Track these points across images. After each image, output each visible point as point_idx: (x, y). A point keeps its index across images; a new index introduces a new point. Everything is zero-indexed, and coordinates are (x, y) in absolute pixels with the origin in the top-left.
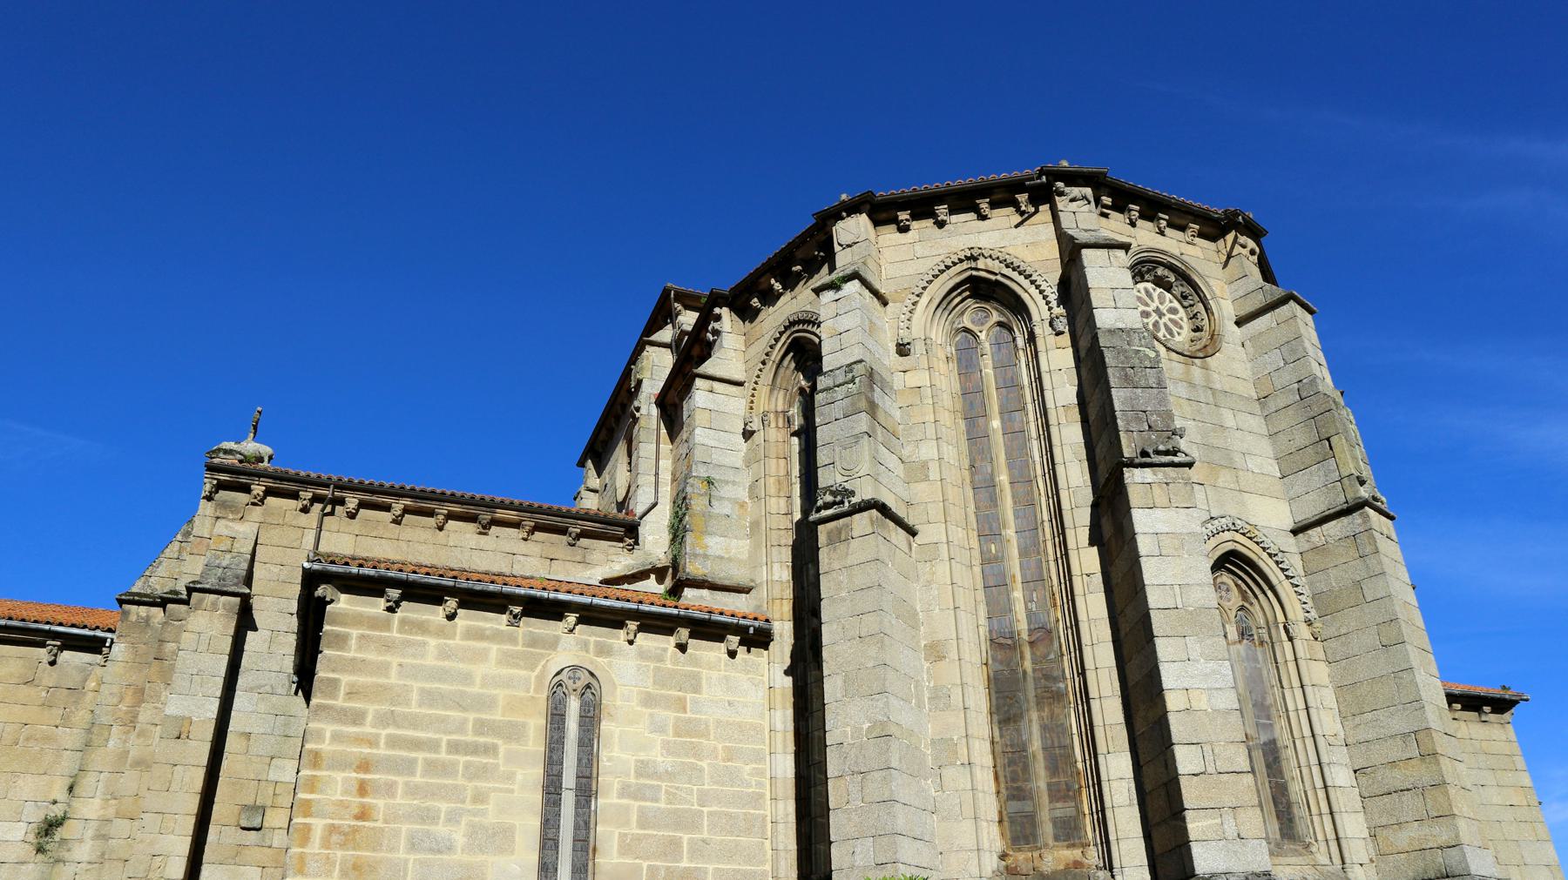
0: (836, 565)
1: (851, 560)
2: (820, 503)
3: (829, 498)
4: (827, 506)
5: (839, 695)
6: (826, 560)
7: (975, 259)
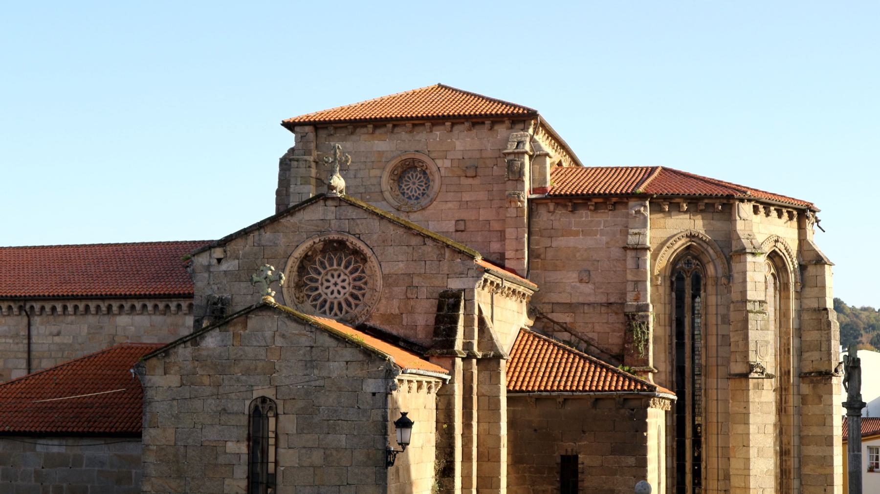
0: (757, 400)
1: (763, 399)
2: (755, 371)
3: (758, 370)
4: (756, 372)
5: (756, 456)
6: (753, 396)
7: (776, 241)
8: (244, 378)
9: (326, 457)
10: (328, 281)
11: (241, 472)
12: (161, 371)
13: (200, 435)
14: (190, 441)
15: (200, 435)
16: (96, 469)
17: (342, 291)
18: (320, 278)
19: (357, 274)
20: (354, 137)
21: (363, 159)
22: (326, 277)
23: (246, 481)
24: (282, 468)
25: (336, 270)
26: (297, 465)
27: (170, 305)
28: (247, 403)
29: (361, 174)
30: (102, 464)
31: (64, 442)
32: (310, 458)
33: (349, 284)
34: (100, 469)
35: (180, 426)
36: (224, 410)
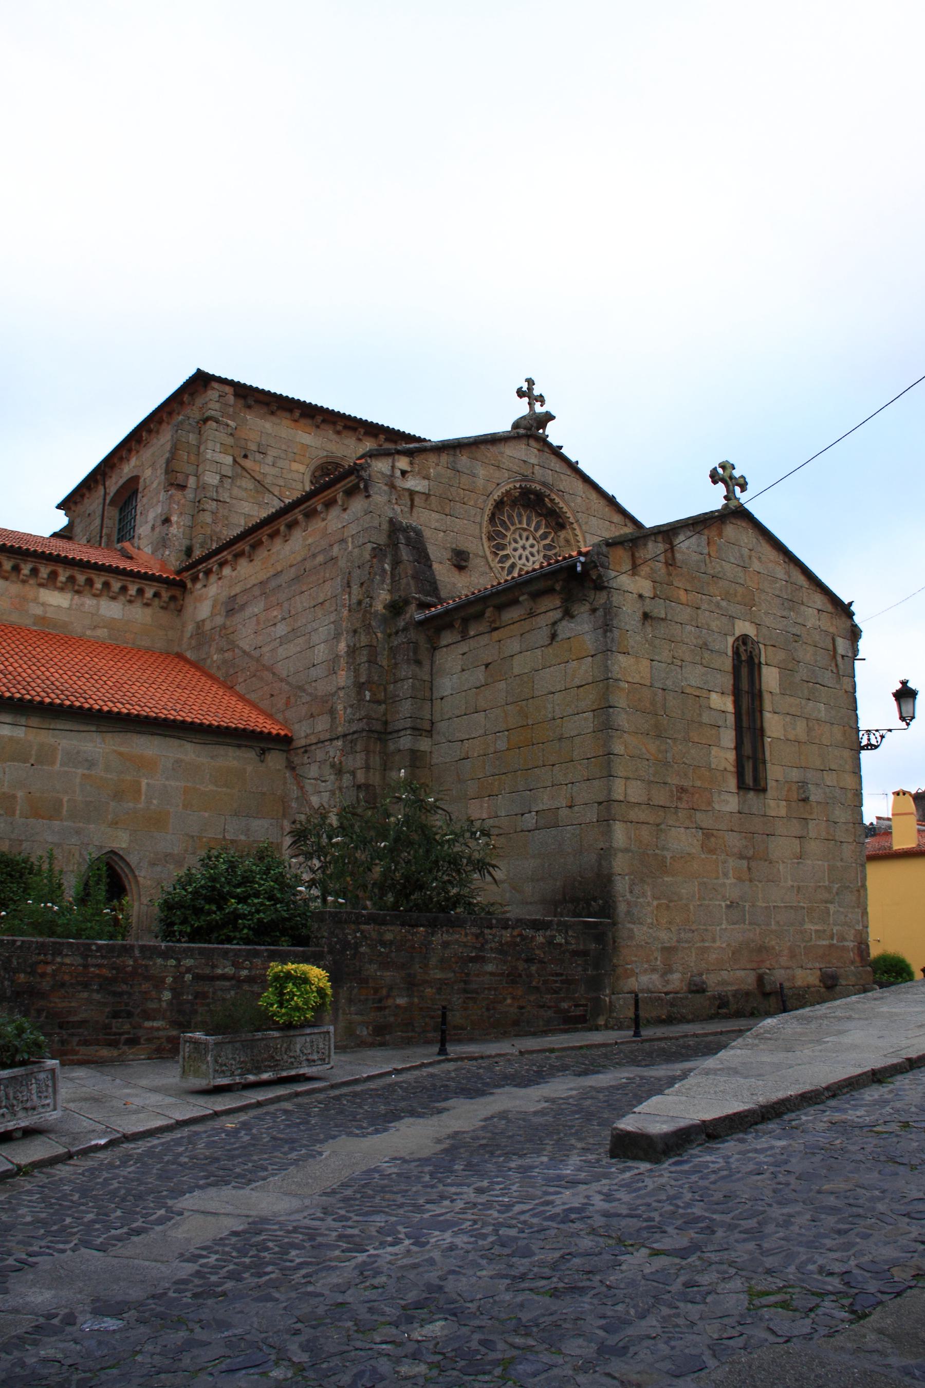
8: (724, 604)
9: (809, 730)
10: (516, 542)
11: (728, 738)
12: (627, 566)
13: (680, 677)
14: (669, 683)
15: (680, 677)
16: (80, 771)
17: (532, 559)
18: (508, 534)
19: (547, 542)
20: (274, 419)
21: (284, 447)
22: (514, 536)
23: (734, 752)
24: (769, 740)
25: (525, 530)
26: (782, 738)
27: (23, 566)
28: (731, 640)
29: (280, 463)
30: (91, 764)
31: (23, 721)
32: (794, 729)
33: (538, 552)
34: (86, 772)
35: (656, 658)
36: (705, 644)
